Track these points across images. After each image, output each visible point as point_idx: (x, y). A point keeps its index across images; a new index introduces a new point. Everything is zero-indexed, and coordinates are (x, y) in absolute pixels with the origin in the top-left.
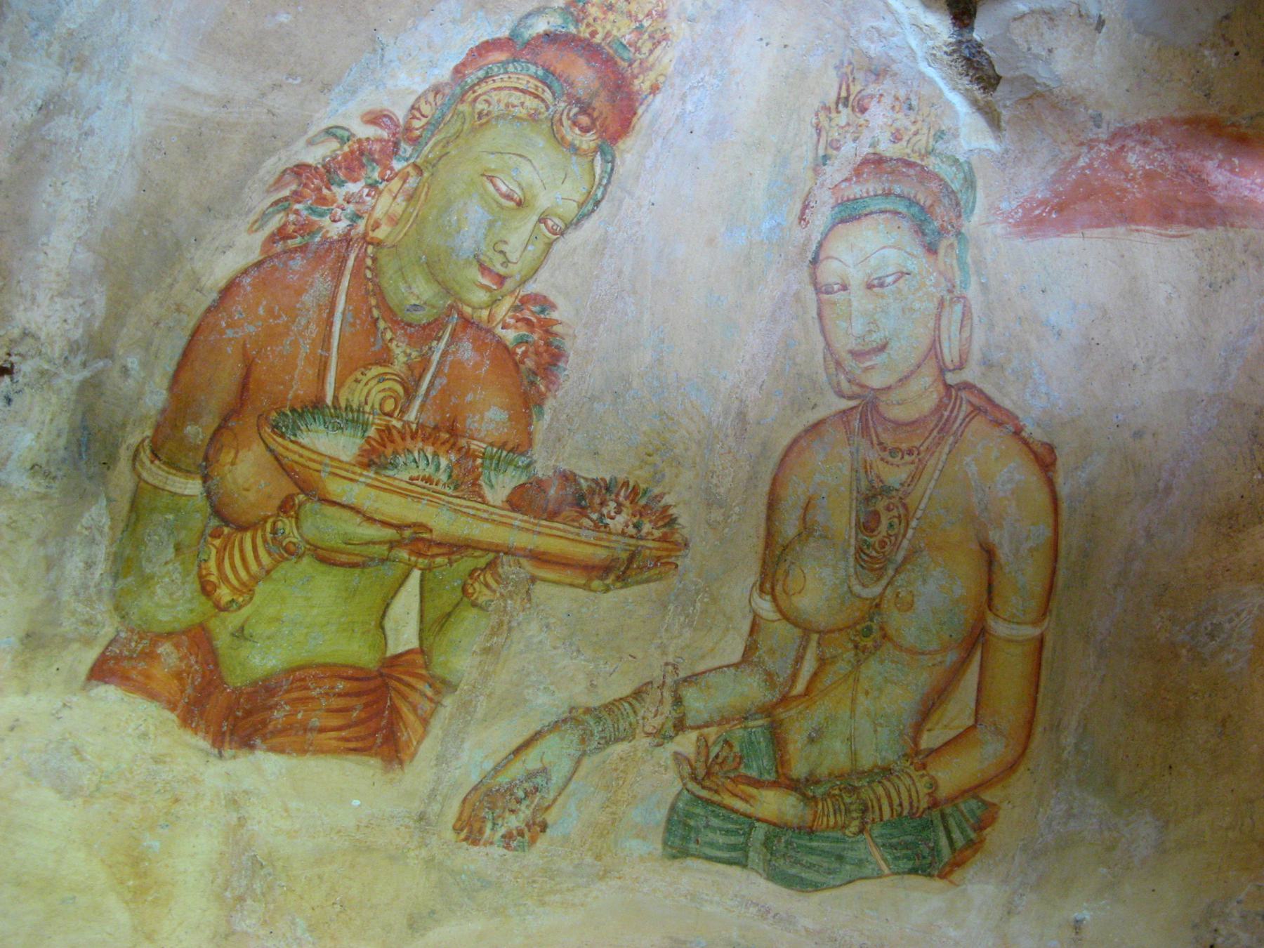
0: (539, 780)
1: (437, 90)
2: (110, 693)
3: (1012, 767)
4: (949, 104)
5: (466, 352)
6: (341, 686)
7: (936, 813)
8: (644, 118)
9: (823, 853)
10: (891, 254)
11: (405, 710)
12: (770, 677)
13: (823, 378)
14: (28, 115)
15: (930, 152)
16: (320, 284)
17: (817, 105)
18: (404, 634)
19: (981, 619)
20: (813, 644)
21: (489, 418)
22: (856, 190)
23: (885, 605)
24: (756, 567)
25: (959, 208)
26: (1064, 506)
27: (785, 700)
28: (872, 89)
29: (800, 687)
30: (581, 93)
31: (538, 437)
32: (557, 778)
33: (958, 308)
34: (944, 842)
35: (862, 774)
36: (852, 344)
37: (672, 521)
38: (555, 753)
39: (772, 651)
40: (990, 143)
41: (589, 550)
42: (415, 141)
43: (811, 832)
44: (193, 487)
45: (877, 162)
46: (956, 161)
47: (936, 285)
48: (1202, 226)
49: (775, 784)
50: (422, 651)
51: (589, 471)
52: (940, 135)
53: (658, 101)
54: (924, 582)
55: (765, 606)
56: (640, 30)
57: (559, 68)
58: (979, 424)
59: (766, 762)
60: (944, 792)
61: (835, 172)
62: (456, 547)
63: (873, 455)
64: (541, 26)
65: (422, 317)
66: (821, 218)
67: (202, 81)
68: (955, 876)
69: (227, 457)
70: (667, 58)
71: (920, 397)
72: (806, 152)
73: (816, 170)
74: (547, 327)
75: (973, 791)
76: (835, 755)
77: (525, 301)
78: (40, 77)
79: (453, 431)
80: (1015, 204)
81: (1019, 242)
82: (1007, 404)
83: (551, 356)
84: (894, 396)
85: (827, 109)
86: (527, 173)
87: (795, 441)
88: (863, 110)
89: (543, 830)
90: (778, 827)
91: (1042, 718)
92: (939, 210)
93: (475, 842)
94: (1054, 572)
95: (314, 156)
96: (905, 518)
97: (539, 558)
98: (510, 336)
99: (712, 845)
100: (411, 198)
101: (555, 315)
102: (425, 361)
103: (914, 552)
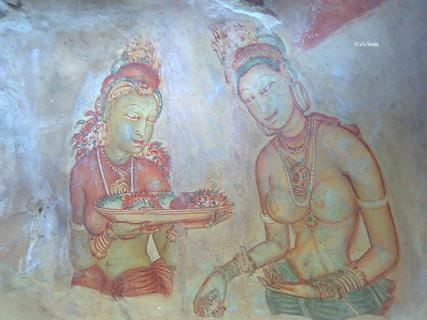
0: (216, 293)
1: (99, 98)
2: (77, 287)
3: (396, 263)
4: (254, 18)
5: (140, 167)
6: (142, 274)
7: (368, 286)
8: (162, 77)
9: (329, 308)
10: (264, 78)
11: (164, 278)
12: (280, 245)
13: (260, 133)
14: (14, 150)
15: (258, 37)
16: (93, 163)
17: (210, 44)
18: (155, 256)
19: (357, 203)
20: (291, 229)
21: (155, 184)
22: (240, 63)
23: (313, 208)
24: (259, 206)
25: (280, 50)
26: (372, 148)
27: (288, 251)
28: (225, 28)
29: (292, 245)
30: (139, 78)
31: (172, 185)
32: (221, 292)
33: (297, 86)
34: (377, 299)
35: (331, 274)
36: (265, 116)
37: (225, 198)
38: (216, 282)
39: (276, 235)
40: (278, 22)
41: (202, 215)
42: (101, 115)
43: (321, 299)
44: (82, 228)
45: (241, 51)
46: (269, 36)
47: (285, 82)
48: (375, 6)
49: (299, 283)
50: (162, 258)
51: (191, 190)
52: (257, 29)
53: (162, 68)
54: (325, 194)
55: (267, 219)
56: (146, 51)
57: (130, 75)
58: (322, 127)
59: (292, 275)
60: (369, 278)
61: (229, 61)
62: (160, 225)
63: (287, 153)
64: (118, 66)
65: (123, 162)
66: (234, 78)
67: (43, 125)
68: (387, 313)
69: (88, 217)
70: (158, 55)
71: (297, 126)
72: (216, 62)
73: (223, 64)
74: (162, 151)
75: (382, 275)
76: (317, 268)
77: (152, 145)
78: (11, 141)
79: (145, 191)
80: (299, 38)
81: (309, 52)
82: (331, 115)
83: (166, 159)
84: (287, 129)
85: (214, 43)
86: (137, 109)
87: (259, 157)
88: (226, 36)
89: (225, 309)
90: (308, 299)
91: (402, 239)
92: (273, 55)
93: (203, 316)
94: (381, 175)
95: (77, 131)
96: (308, 172)
97: (186, 222)
98: (151, 158)
99: (286, 308)
100: (107, 130)
101: (163, 146)
102: (129, 174)
103: (316, 185)
